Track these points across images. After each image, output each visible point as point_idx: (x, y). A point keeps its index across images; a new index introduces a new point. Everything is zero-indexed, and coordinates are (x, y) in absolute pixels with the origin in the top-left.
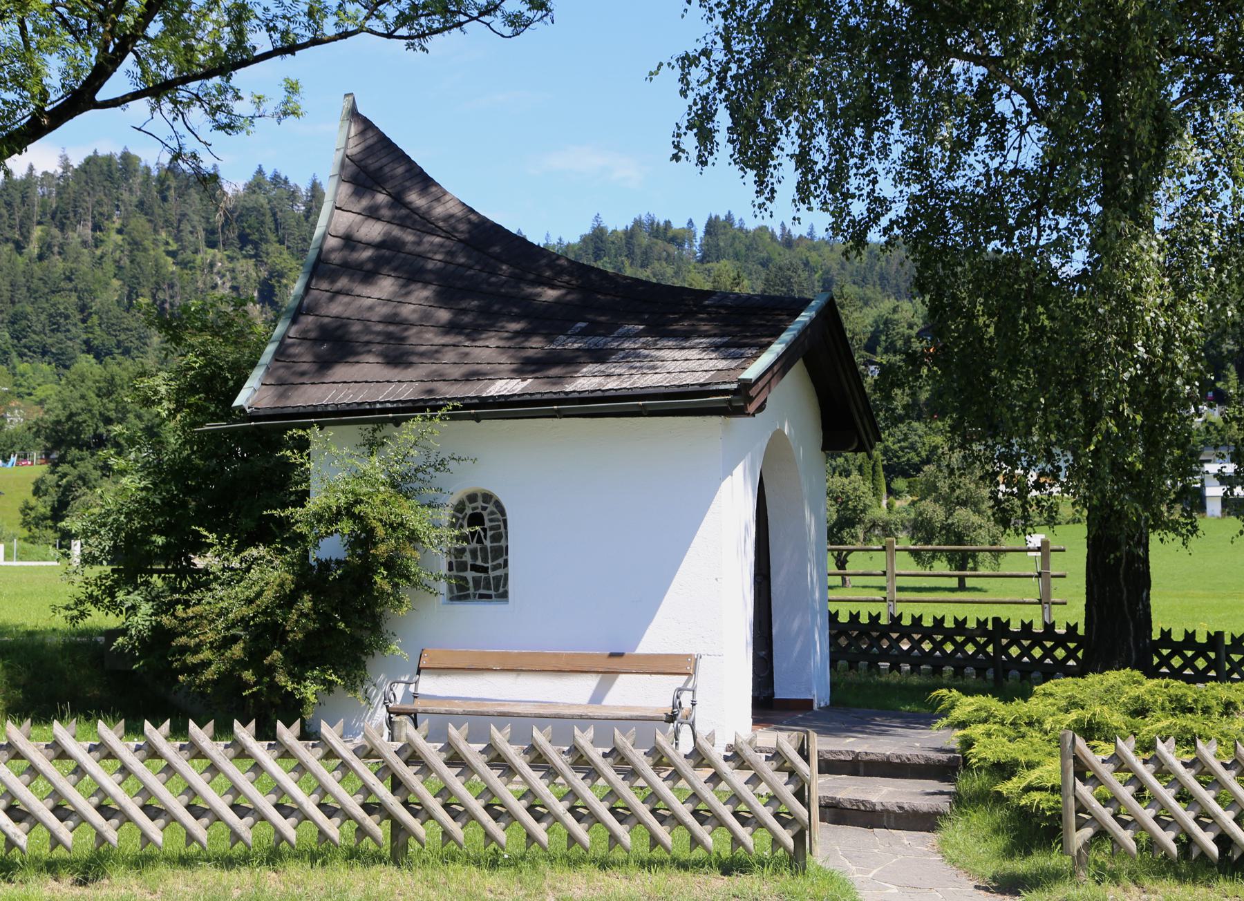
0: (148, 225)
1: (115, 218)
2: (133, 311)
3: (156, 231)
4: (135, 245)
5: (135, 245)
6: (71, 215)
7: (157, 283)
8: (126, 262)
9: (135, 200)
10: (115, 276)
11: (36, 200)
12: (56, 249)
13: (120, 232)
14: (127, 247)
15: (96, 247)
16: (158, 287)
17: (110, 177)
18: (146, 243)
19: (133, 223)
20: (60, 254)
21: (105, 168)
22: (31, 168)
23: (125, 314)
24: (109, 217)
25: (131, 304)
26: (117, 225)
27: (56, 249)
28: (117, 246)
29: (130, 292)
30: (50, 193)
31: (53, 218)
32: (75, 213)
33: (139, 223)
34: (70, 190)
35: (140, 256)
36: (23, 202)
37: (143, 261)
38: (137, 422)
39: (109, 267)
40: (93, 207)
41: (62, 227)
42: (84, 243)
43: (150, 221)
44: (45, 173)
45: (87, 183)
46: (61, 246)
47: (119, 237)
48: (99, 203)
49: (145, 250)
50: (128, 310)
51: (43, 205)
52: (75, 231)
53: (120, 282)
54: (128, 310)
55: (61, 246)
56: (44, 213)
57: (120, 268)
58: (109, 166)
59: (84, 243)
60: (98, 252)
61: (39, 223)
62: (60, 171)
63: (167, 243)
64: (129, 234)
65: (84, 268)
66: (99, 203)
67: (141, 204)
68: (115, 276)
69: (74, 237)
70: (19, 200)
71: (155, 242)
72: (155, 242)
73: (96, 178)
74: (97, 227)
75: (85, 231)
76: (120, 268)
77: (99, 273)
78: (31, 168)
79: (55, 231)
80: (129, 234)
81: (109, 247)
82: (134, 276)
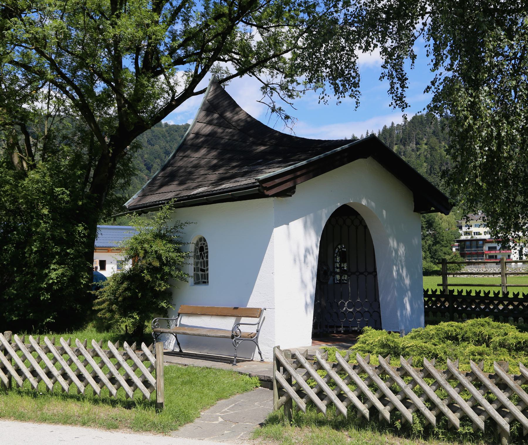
0: (437, 141)
1: (424, 139)
2: (432, 175)
3: (440, 142)
4: (432, 149)
5: (432, 149)
6: (408, 140)
7: (441, 163)
8: (429, 156)
9: (431, 131)
10: (425, 162)
11: (395, 135)
12: (402, 154)
13: (426, 144)
14: (429, 150)
15: (417, 151)
16: (441, 164)
17: (421, 123)
18: (436, 147)
19: (431, 140)
20: (404, 155)
21: (420, 120)
22: (393, 123)
23: (429, 177)
24: (422, 139)
25: (431, 172)
26: (425, 142)
27: (402, 154)
28: (426, 150)
29: (431, 167)
30: (400, 132)
31: (401, 142)
32: (409, 139)
33: (434, 140)
34: (407, 130)
35: (434, 153)
36: (390, 137)
37: (435, 155)
38: (423, 219)
39: (422, 158)
40: (416, 135)
41: (404, 145)
42: (413, 150)
43: (437, 139)
44: (398, 125)
45: (413, 127)
46: (404, 152)
47: (426, 146)
48: (418, 134)
49: (436, 150)
50: (430, 175)
51: (397, 137)
52: (409, 146)
53: (427, 164)
54: (430, 175)
55: (404, 152)
56: (398, 140)
57: (426, 158)
58: (421, 119)
59: (413, 150)
60: (418, 153)
61: (396, 144)
62: (403, 123)
63: (445, 147)
64: (430, 145)
65: (413, 160)
66: (418, 134)
67: (434, 132)
68: (425, 162)
69: (409, 148)
70: (388, 136)
71: (440, 147)
72: (440, 147)
73: (417, 124)
74: (417, 143)
75: (413, 145)
76: (426, 158)
77: (418, 161)
78: (393, 123)
79: (402, 147)
80: (430, 145)
81: (422, 151)
82: (432, 161)
